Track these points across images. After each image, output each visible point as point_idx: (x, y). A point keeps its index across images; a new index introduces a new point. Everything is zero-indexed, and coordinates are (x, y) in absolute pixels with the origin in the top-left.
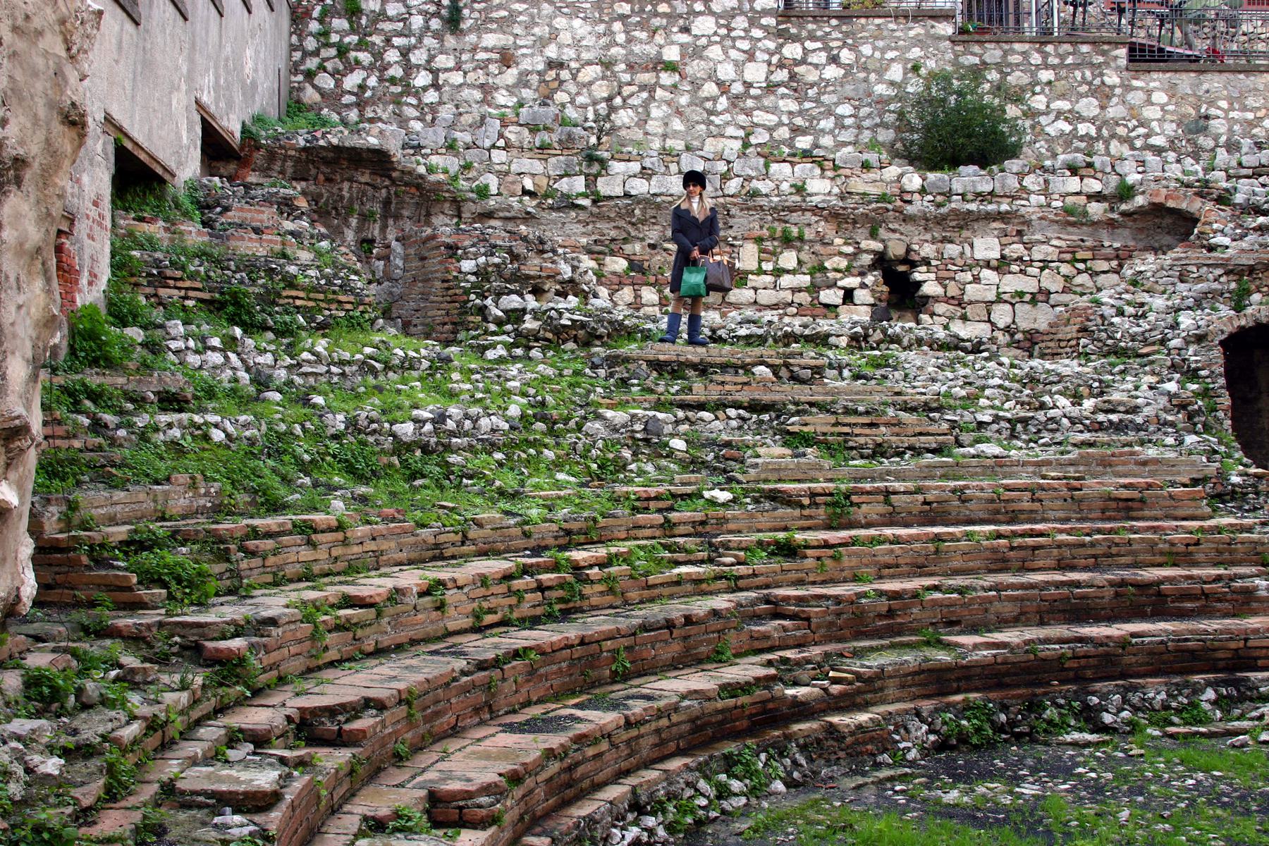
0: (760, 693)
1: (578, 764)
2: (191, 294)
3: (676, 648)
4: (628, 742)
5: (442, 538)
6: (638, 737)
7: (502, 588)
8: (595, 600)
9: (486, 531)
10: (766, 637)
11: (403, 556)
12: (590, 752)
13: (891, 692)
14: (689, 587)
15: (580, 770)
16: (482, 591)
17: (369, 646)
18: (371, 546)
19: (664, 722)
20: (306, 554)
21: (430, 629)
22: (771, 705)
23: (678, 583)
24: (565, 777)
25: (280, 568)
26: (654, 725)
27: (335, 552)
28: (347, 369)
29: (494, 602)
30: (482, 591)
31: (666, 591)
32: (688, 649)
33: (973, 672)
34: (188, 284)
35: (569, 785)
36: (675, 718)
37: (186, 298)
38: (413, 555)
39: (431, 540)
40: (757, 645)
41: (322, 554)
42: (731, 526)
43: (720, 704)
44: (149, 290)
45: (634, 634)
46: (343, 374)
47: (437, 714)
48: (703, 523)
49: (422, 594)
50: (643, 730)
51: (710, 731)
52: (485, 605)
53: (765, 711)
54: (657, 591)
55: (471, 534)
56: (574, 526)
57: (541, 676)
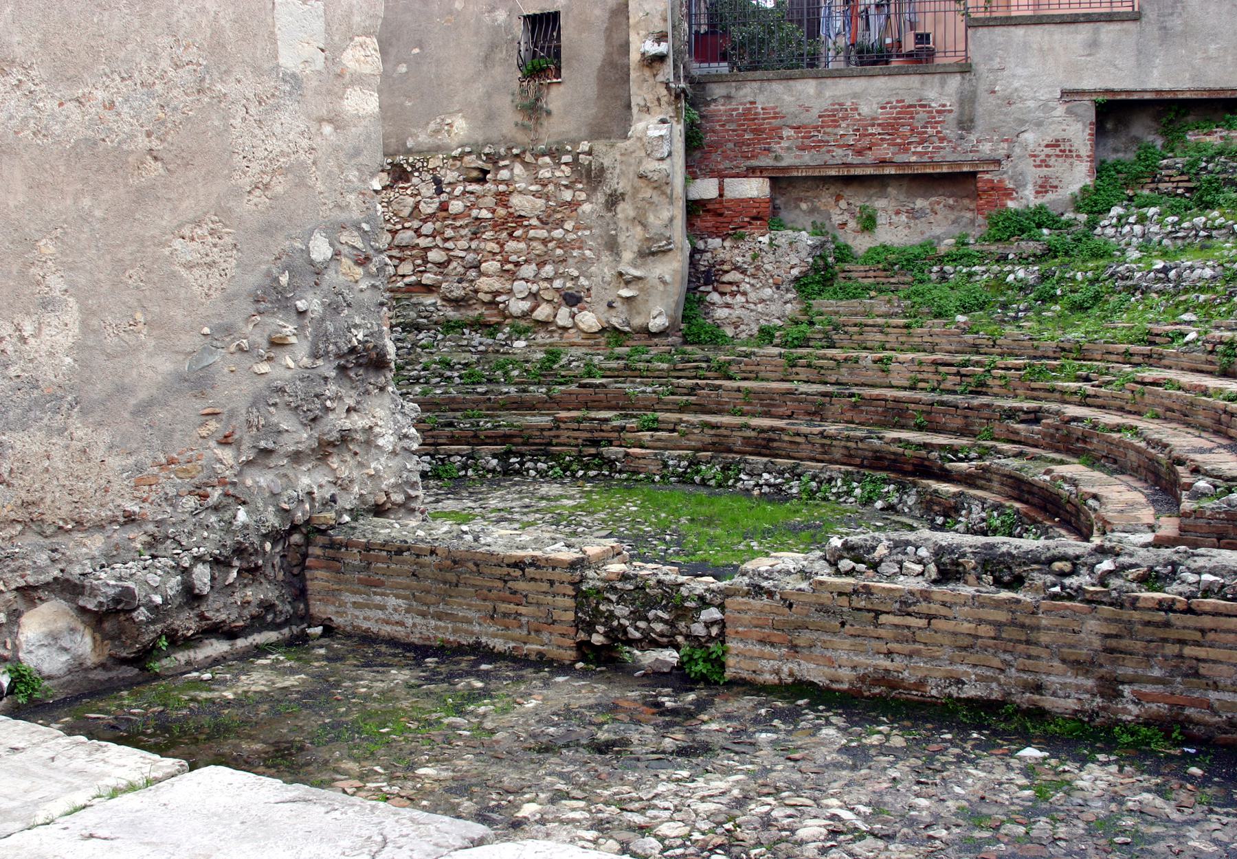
0: (923, 453)
1: (775, 440)
2: (1180, 184)
3: (958, 422)
4: (823, 445)
5: (978, 342)
6: (830, 445)
7: (932, 369)
8: (996, 390)
9: (1009, 341)
10: (1016, 433)
11: (953, 348)
12: (786, 438)
13: (996, 485)
14: (1057, 395)
15: (775, 444)
16: (917, 368)
17: (833, 379)
18: (929, 339)
19: (853, 445)
20: (879, 337)
21: (878, 381)
22: (926, 463)
23: (1048, 390)
24: (764, 443)
25: (863, 341)
26: (843, 443)
27: (901, 339)
28: (1214, 233)
29: (925, 376)
30: (917, 368)
31: (1042, 394)
32: (967, 425)
33: (1035, 490)
34: (1178, 178)
35: (765, 447)
36: (860, 445)
37: (1177, 188)
38: (959, 348)
39: (971, 341)
40: (1012, 437)
41: (892, 338)
42: (1165, 362)
43: (894, 448)
44: (1152, 186)
45: (932, 404)
46: (1209, 237)
47: (774, 406)
48: (1150, 356)
49: (875, 362)
50: (834, 443)
51: (887, 463)
52: (920, 376)
53: (922, 465)
54: (1035, 394)
55: (998, 342)
56: (1067, 345)
57: (862, 411)
